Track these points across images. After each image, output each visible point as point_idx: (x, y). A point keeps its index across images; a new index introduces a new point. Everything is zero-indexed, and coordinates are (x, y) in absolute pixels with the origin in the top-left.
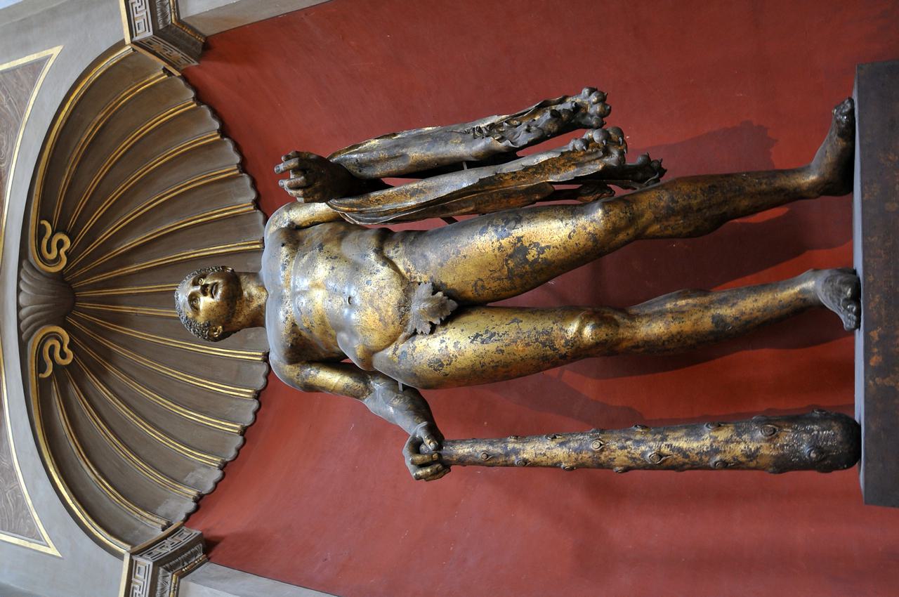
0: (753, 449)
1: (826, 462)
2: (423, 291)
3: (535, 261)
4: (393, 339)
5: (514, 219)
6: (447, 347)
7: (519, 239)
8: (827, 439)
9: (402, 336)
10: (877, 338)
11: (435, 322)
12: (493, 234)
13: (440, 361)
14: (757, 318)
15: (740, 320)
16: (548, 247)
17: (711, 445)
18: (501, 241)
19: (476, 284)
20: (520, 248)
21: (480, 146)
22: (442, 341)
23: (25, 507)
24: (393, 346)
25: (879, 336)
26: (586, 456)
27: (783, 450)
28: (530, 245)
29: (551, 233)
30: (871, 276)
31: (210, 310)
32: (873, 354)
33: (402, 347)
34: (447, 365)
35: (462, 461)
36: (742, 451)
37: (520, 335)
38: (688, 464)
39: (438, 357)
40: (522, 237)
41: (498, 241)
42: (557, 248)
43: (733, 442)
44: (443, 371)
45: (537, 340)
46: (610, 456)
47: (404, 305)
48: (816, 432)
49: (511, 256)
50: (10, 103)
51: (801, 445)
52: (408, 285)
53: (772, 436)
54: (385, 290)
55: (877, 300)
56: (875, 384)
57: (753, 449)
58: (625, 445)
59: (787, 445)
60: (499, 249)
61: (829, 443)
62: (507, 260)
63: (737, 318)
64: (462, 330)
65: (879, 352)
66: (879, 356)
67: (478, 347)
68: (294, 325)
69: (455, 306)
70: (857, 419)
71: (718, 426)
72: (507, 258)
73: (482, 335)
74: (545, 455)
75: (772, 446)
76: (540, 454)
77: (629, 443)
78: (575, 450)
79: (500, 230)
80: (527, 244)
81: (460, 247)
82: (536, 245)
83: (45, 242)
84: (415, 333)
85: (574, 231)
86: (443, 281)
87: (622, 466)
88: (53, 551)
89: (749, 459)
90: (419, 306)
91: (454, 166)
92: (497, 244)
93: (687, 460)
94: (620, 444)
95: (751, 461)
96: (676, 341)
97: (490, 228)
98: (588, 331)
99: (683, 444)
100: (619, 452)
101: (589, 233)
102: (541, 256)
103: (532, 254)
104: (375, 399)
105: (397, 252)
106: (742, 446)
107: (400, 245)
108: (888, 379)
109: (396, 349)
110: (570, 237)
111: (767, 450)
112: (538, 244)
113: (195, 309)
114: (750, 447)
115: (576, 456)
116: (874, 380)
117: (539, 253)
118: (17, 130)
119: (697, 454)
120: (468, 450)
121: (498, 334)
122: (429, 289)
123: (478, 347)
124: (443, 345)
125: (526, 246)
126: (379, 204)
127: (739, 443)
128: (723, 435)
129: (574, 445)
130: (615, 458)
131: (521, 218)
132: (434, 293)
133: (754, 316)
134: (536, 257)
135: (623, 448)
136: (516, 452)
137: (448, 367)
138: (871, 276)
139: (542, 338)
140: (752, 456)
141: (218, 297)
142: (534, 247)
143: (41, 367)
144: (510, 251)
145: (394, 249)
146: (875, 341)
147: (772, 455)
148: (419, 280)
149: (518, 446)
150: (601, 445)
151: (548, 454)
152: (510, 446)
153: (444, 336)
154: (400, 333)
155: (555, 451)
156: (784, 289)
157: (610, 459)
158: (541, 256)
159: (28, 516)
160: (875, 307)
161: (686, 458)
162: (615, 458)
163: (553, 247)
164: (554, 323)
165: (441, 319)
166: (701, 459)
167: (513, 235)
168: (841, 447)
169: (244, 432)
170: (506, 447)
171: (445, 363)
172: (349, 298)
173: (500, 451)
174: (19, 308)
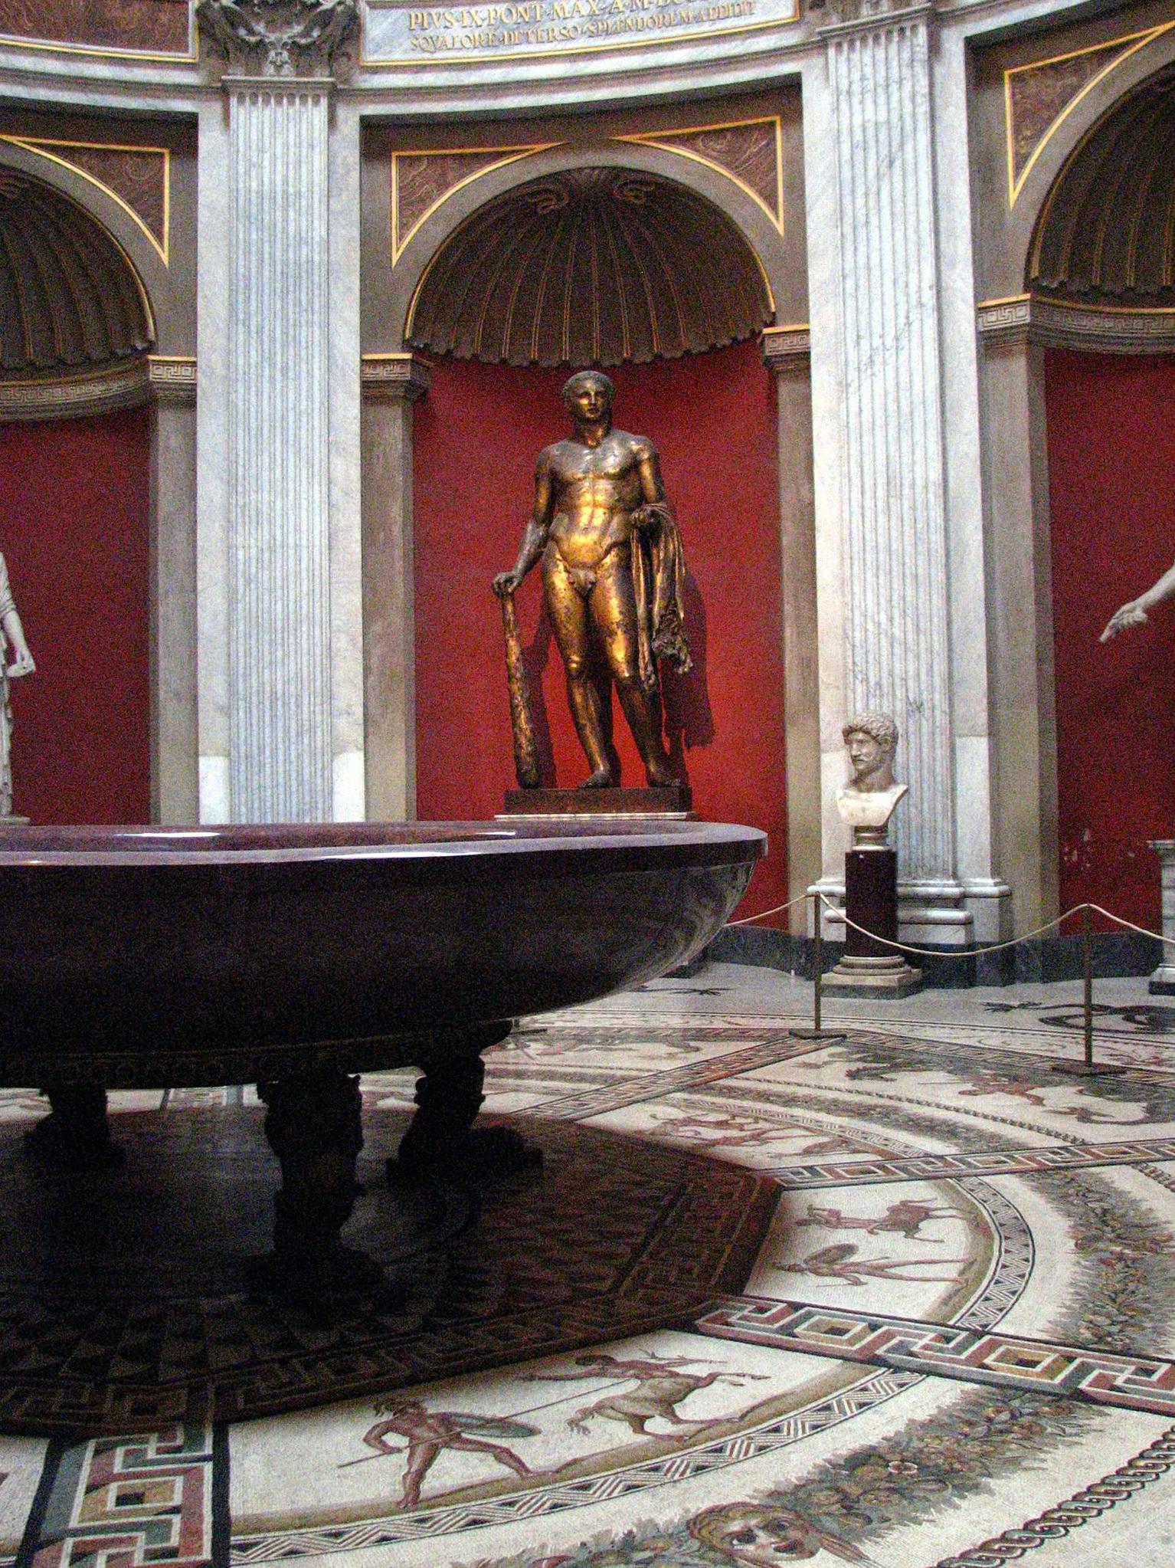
1: (520, 776)
2: (592, 576)
4: (565, 559)
20: (612, 634)
21: (657, 620)
23: (421, 212)
26: (513, 671)
29: (619, 652)
31: (579, 406)
33: (561, 567)
35: (504, 608)
47: (584, 566)
50: (749, 158)
52: (596, 565)
53: (529, 754)
67: (563, 611)
69: (585, 594)
71: (532, 731)
83: (638, 187)
88: (395, 257)
91: (650, 601)
98: (574, 665)
99: (523, 716)
103: (609, 640)
111: (523, 752)
113: (581, 396)
118: (728, 165)
123: (563, 611)
128: (528, 733)
140: (520, 746)
141: (588, 415)
143: (531, 195)
156: (601, 756)
159: (415, 217)
174: (580, 170)
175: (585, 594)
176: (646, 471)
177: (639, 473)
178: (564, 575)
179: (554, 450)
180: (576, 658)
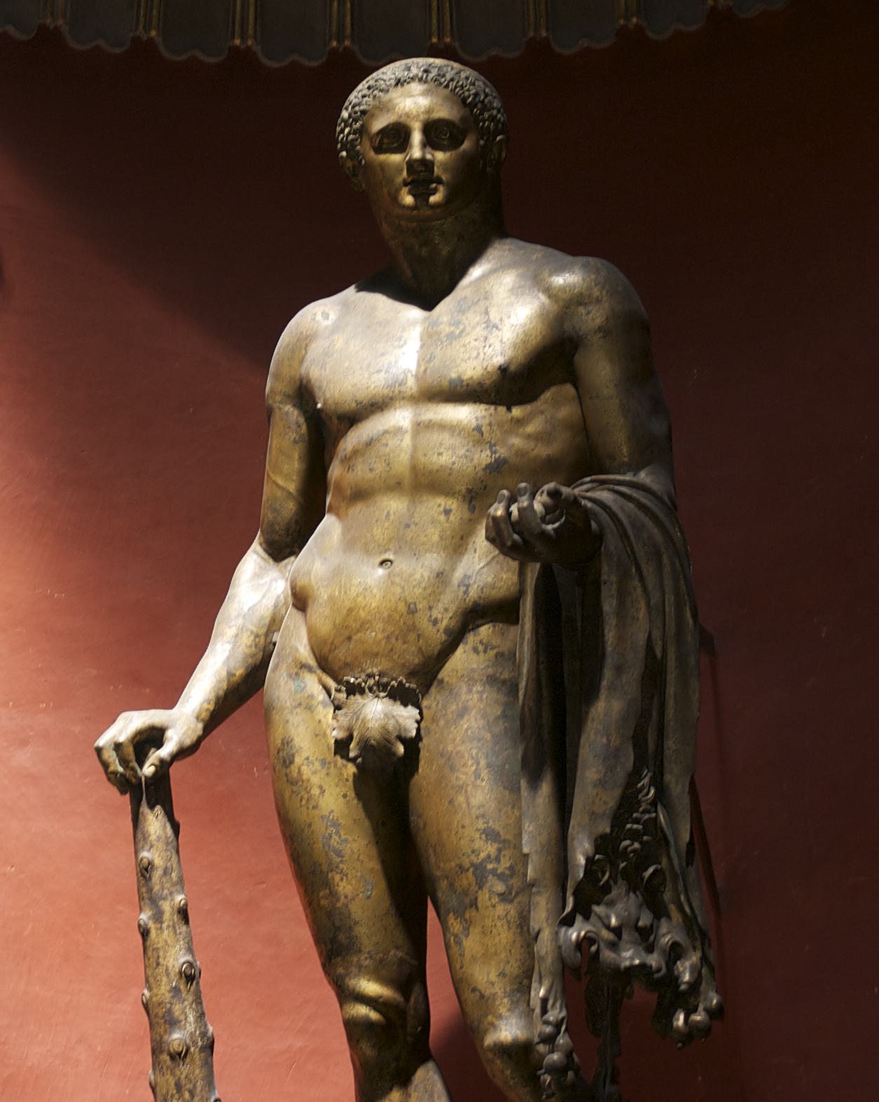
5: (510, 889)
6: (315, 772)
7: (474, 904)
11: (352, 746)
12: (482, 855)
13: (292, 762)
18: (471, 870)
22: (323, 762)
24: (312, 662)
28: (466, 921)
34: (286, 775)
39: (298, 760)
40: (477, 908)
41: (472, 864)
45: (338, 929)
49: (451, 885)
54: (400, 641)
58: (183, 1089)
60: (460, 867)
62: (447, 877)
64: (345, 796)
68: (352, 418)
69: (387, 777)
73: (337, 833)
74: (158, 964)
77: (187, 1095)
78: (169, 1011)
79: (490, 866)
80: (467, 916)
81: (466, 791)
84: (338, 708)
85: (482, 996)
86: (424, 754)
90: (377, 712)
92: (466, 864)
94: (183, 1082)
97: (496, 846)
100: (172, 1082)
101: (479, 1022)
104: (257, 576)
105: (475, 650)
107: (492, 653)
109: (310, 669)
110: (474, 990)
112: (467, 936)
115: (160, 1014)
117: (456, 936)
120: (152, 832)
121: (341, 862)
122: (405, 730)
124: (317, 765)
125: (464, 913)
129: (177, 1010)
131: (511, 901)
132: (401, 738)
135: (178, 1086)
136: (158, 917)
139: (342, 937)
145: (481, 642)
148: (425, 703)
149: (167, 916)
150: (180, 1054)
151: (161, 970)
152: (166, 907)
153: (332, 765)
155: (165, 979)
158: (452, 939)
164: (369, 953)
167: (480, 892)
169: (240, 57)
170: (165, 899)
173: (156, 888)
175: (387, 777)
176: (601, 369)
177: (572, 376)
178: (326, 714)
179: (319, 316)
180: (371, 987)
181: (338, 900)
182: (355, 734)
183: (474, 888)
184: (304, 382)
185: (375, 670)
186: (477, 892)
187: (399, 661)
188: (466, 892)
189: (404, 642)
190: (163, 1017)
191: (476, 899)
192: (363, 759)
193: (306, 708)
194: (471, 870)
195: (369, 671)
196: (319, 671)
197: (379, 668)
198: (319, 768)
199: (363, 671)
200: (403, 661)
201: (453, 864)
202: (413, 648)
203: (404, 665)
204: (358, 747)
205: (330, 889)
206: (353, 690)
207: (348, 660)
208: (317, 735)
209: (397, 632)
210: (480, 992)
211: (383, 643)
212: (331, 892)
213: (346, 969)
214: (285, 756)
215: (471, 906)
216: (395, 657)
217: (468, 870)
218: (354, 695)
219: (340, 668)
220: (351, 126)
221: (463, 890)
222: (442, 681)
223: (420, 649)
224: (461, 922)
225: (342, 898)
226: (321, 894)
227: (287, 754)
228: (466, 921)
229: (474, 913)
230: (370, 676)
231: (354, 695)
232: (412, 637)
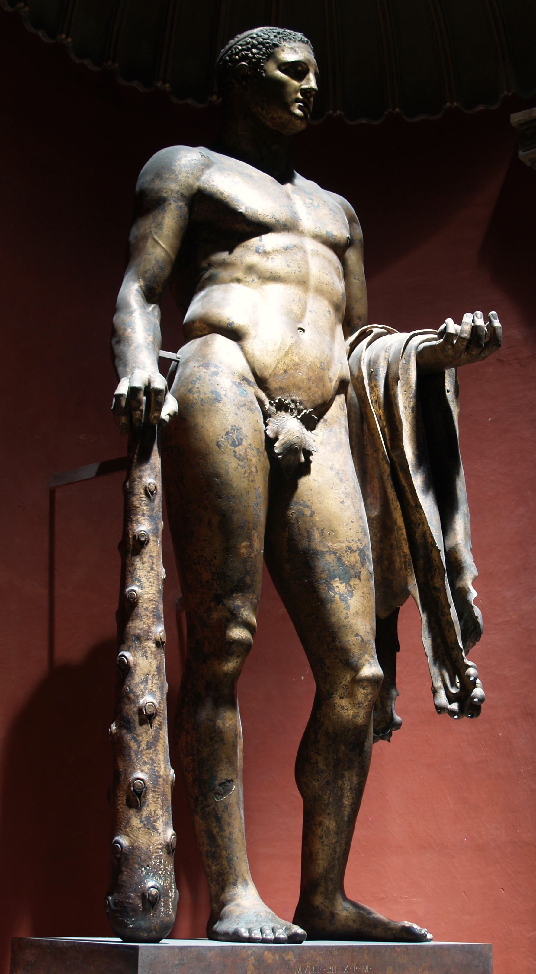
0: (156, 824)
3: (331, 588)
6: (254, 456)
7: (358, 576)
8: (166, 906)
9: (263, 396)
10: (287, 958)
14: (222, 829)
15: (224, 811)
16: (348, 608)
17: (160, 777)
18: (358, 552)
19: (308, 507)
25: (289, 960)
27: (155, 858)
28: (350, 586)
30: (337, 953)
32: (274, 955)
34: (234, 451)
36: (155, 812)
37: (255, 553)
38: (139, 747)
40: (360, 579)
42: (345, 618)
43: (162, 801)
44: (226, 444)
45: (247, 572)
46: (149, 652)
48: (170, 895)
49: (339, 559)
51: (161, 878)
55: (318, 959)
56: (249, 956)
57: (156, 824)
59: (161, 863)
60: (350, 548)
61: (162, 909)
62: (335, 553)
63: (227, 808)
65: (276, 960)
66: (273, 960)
70: (163, 941)
72: (338, 554)
75: (160, 847)
76: (153, 563)
80: (352, 583)
82: (351, 593)
87: (135, 665)
89: (143, 819)
93: (143, 746)
95: (141, 822)
96: (213, 735)
102: (337, 596)
106: (160, 812)
108: (252, 968)
110: (357, 635)
112: (352, 596)
114: (158, 822)
116: (252, 955)
117: (341, 595)
119: (152, 759)
125: (349, 580)
126: (405, 407)
127: (162, 809)
130: (147, 657)
133: (226, 828)
134: (337, 590)
137: (232, 454)
138: (337, 953)
139: (248, 579)
142: (349, 591)
144: (345, 560)
146: (284, 956)
147: (150, 846)
154: (269, 396)
157: (146, 652)
160: (312, 956)
161: (147, 746)
162: (147, 657)
163: (347, 613)
165: (279, 454)
166: (145, 763)
168: (159, 921)
171: (237, 449)
172: (304, 330)
181: (253, 551)
182: (280, 437)
183: (359, 565)
184: (185, 192)
185: (297, 399)
186: (360, 568)
187: (312, 397)
188: (352, 567)
189: (316, 387)
190: (153, 611)
191: (360, 572)
192: (283, 456)
193: (249, 409)
194: (358, 552)
195: (294, 398)
196: (256, 387)
197: (300, 398)
198: (256, 454)
199: (290, 396)
200: (313, 399)
201: (344, 545)
202: (320, 393)
203: (313, 401)
204: (281, 448)
205: (250, 542)
206: (282, 407)
207: (283, 385)
208: (256, 431)
209: (313, 378)
210: (362, 638)
211: (306, 381)
212: (250, 545)
213: (243, 603)
214: (235, 438)
215: (356, 577)
216: (310, 394)
217: (355, 552)
218: (281, 411)
219: (276, 389)
220: (258, 49)
221: (350, 564)
222: (326, 421)
223: (323, 395)
224: (346, 587)
225: (255, 550)
226: (244, 544)
227: (237, 438)
228: (350, 586)
229: (357, 581)
230: (293, 401)
231: (281, 411)
232: (321, 386)
